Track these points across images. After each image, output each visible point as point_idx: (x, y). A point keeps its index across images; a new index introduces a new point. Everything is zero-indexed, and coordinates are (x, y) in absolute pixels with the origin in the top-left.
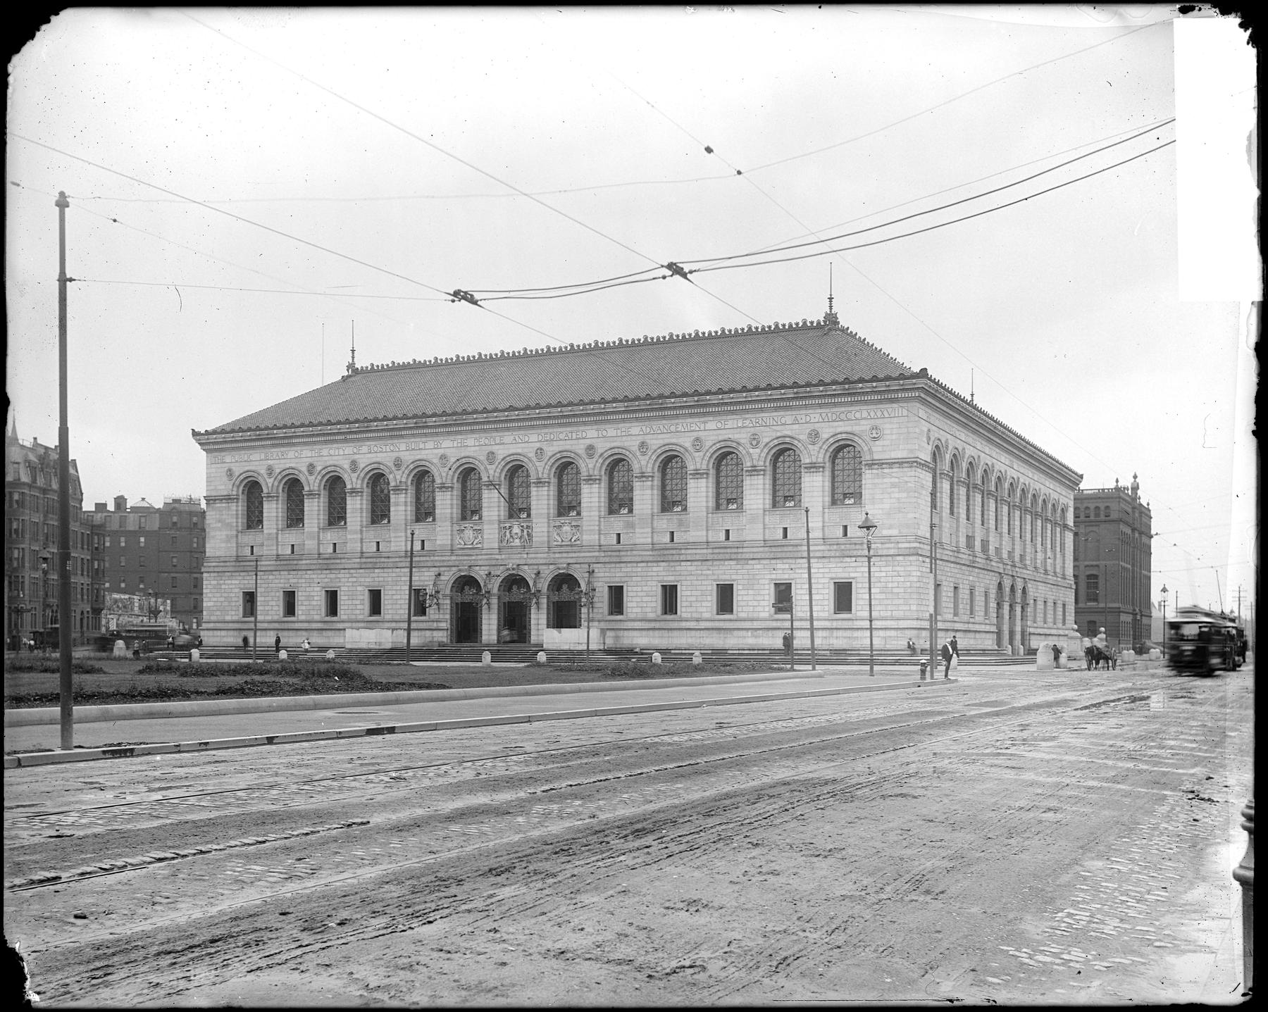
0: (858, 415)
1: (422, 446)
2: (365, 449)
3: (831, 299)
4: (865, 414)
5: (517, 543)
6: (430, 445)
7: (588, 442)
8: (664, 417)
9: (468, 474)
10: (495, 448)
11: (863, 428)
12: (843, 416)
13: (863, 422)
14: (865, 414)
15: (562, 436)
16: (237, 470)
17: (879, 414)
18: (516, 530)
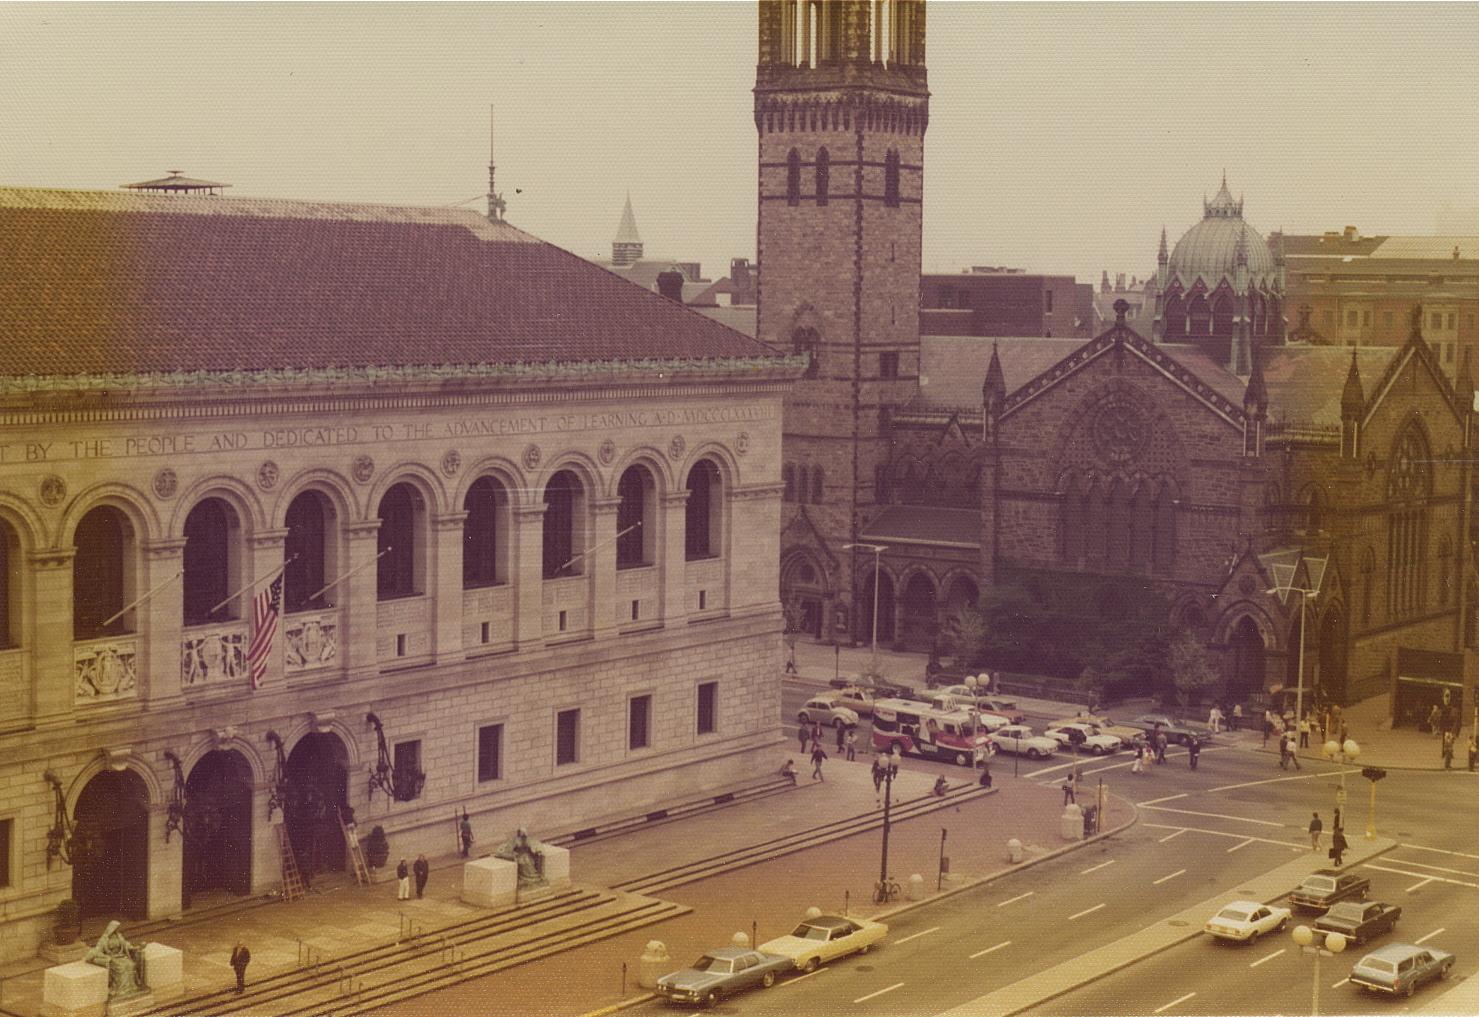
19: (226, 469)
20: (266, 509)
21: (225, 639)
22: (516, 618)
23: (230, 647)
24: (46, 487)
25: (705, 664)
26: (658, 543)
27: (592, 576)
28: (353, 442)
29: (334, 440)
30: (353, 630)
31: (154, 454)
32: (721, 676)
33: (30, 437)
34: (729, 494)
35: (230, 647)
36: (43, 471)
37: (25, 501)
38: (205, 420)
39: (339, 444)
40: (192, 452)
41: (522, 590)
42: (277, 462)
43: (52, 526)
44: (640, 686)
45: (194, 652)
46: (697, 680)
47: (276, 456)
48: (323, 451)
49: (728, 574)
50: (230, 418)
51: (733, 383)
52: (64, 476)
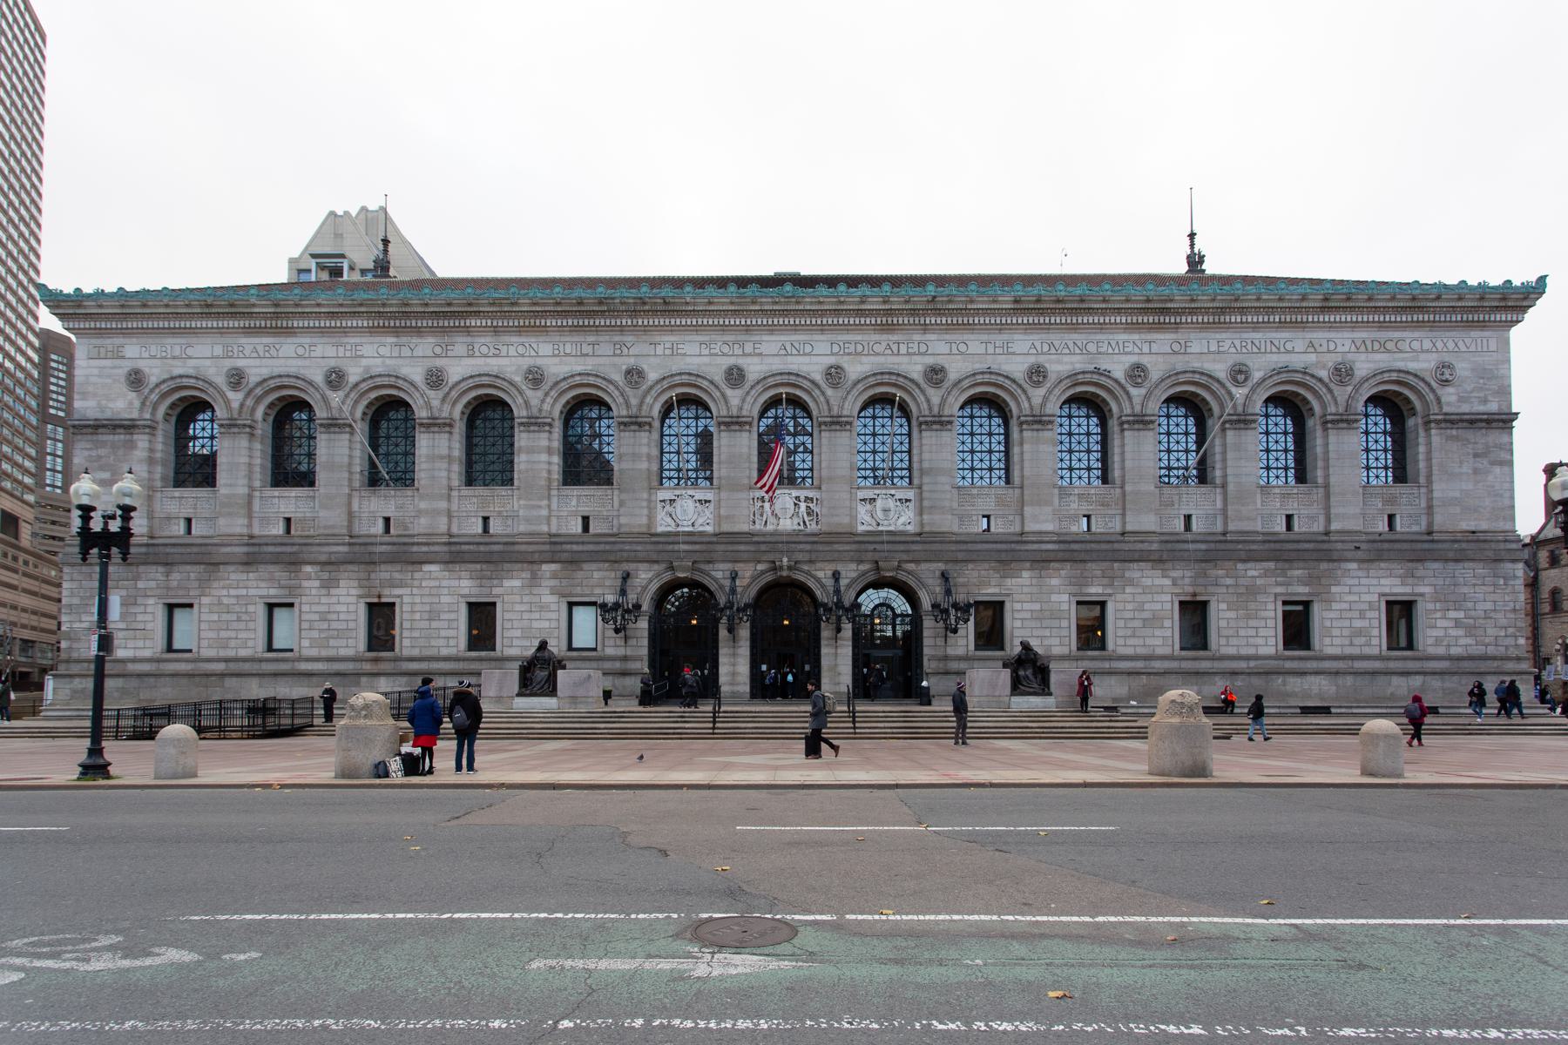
0: (1416, 345)
1: (587, 349)
4: (1427, 345)
6: (606, 349)
7: (930, 360)
8: (1074, 327)
11: (1424, 365)
12: (1390, 345)
13: (1423, 356)
14: (1427, 345)
15: (877, 348)
16: (155, 373)
17: (1451, 345)
20: (832, 401)
21: (797, 498)
22: (1124, 515)
23: (803, 506)
24: (629, 372)
25: (1398, 581)
26: (1320, 464)
27: (1224, 486)
28: (924, 354)
29: (903, 349)
30: (926, 503)
32: (1422, 595)
33: (617, 338)
34: (1427, 423)
35: (803, 506)
36: (626, 362)
37: (610, 382)
38: (772, 329)
39: (908, 354)
41: (1128, 488)
42: (845, 366)
43: (634, 402)
44: (1301, 591)
45: (767, 505)
46: (1381, 595)
47: (845, 362)
48: (891, 359)
49: (1430, 500)
50: (795, 328)
51: (1422, 309)
52: (645, 367)
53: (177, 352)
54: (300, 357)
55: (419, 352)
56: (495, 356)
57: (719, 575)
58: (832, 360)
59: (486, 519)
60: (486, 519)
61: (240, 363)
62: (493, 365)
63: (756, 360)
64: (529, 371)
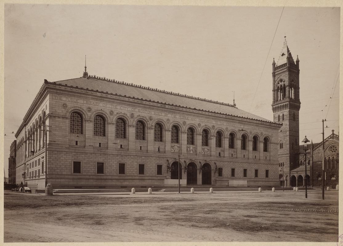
1: (160, 114)
2: (137, 110)
3: (234, 100)
5: (191, 152)
6: (163, 114)
7: (213, 124)
9: (176, 128)
10: (186, 120)
15: (206, 121)
18: (192, 148)
19: (193, 123)
28: (212, 123)
29: (209, 122)
31: (183, 119)
40: (188, 120)
53: (75, 101)
54: (104, 106)
55: (129, 109)
56: (143, 113)
57: (182, 161)
58: (199, 122)
59: (141, 147)
60: (141, 147)
61: (90, 106)
62: (143, 114)
63: (188, 120)
64: (150, 117)
